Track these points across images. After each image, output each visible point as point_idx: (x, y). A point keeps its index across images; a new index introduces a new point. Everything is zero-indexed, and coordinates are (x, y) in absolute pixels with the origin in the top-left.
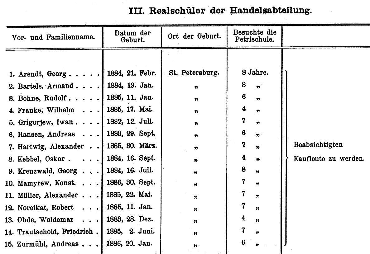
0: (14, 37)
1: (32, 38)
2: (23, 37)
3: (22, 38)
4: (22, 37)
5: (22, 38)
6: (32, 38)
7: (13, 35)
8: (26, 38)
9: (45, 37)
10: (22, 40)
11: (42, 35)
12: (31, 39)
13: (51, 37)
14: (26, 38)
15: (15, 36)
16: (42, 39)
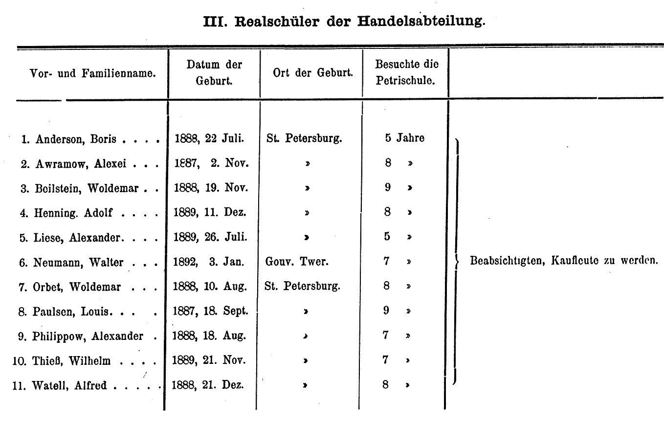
0: (33, 72)
1: (60, 74)
2: (47, 72)
3: (43, 74)
4: (46, 72)
5: (43, 74)
6: (60, 74)
7: (32, 70)
8: (51, 75)
9: (79, 73)
10: (46, 77)
11: (74, 70)
12: (59, 76)
13: (89, 74)
14: (51, 75)
15: (34, 71)
16: (74, 76)
